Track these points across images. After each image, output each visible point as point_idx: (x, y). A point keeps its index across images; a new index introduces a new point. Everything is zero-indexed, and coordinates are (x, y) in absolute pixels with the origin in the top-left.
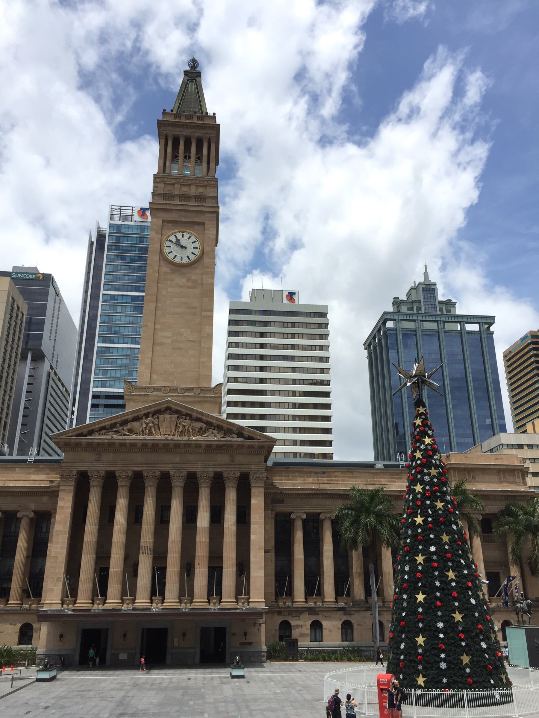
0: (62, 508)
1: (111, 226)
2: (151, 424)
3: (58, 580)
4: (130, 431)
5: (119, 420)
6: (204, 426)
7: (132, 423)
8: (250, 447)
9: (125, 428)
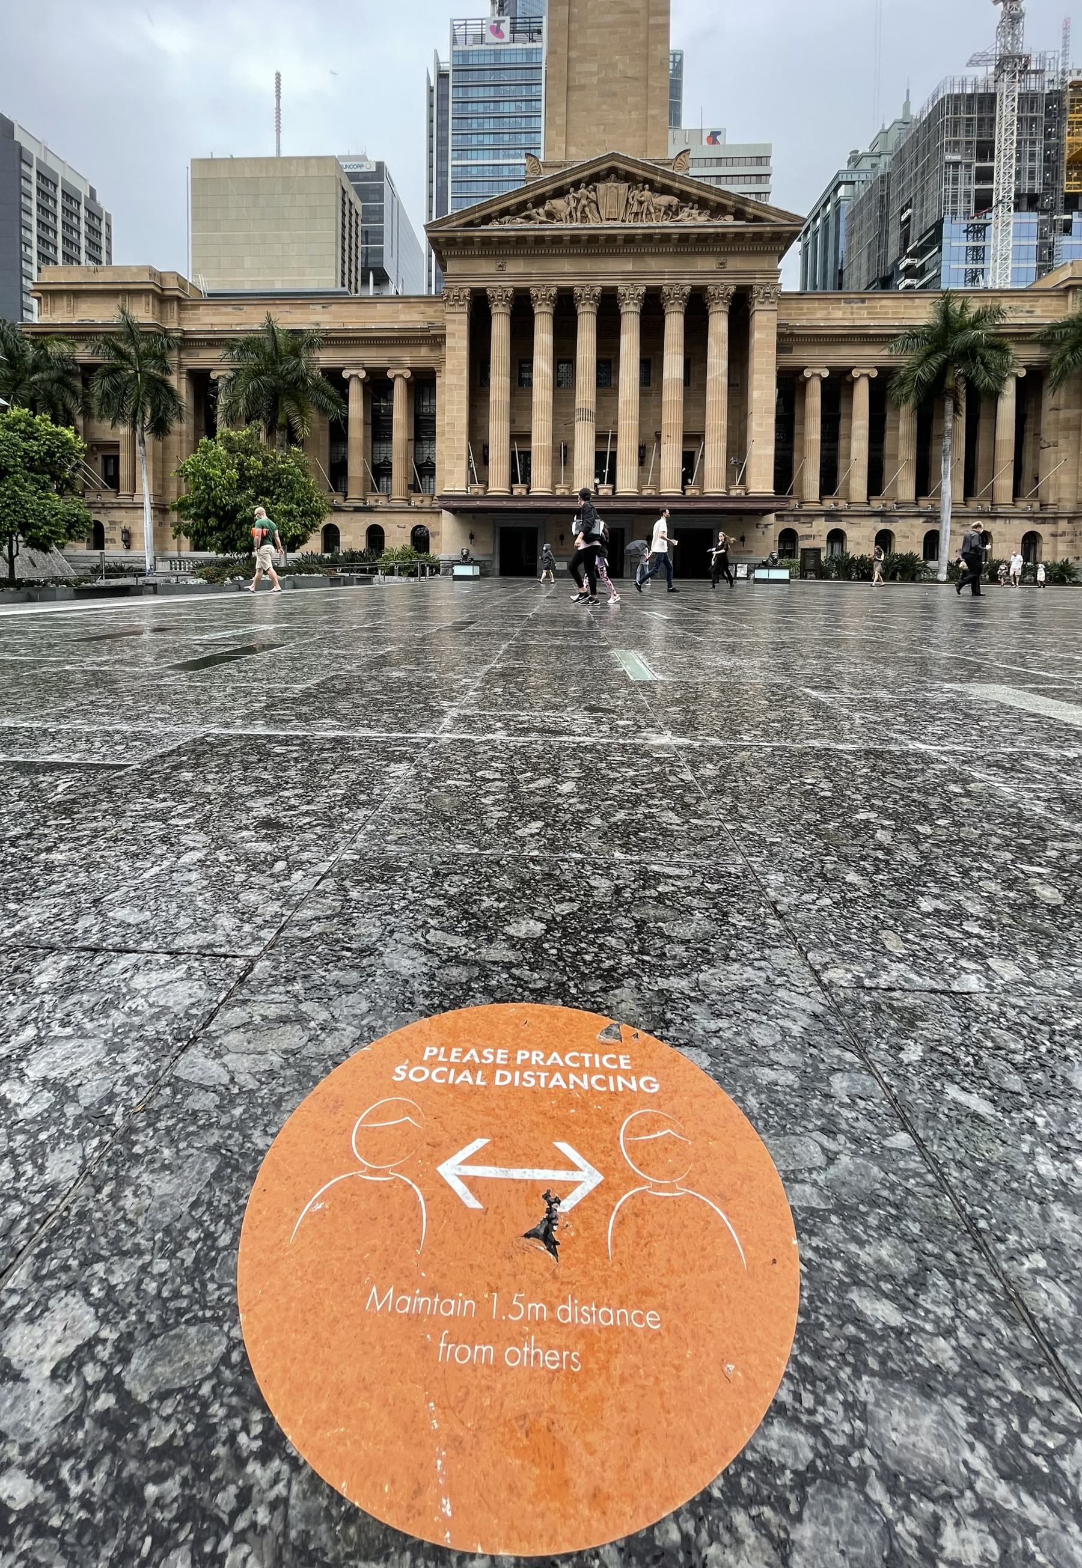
0: (453, 349)
1: (455, 54)
2: (584, 202)
3: (459, 457)
4: (550, 215)
5: (530, 195)
6: (675, 200)
7: (553, 202)
8: (758, 237)
9: (541, 211)
